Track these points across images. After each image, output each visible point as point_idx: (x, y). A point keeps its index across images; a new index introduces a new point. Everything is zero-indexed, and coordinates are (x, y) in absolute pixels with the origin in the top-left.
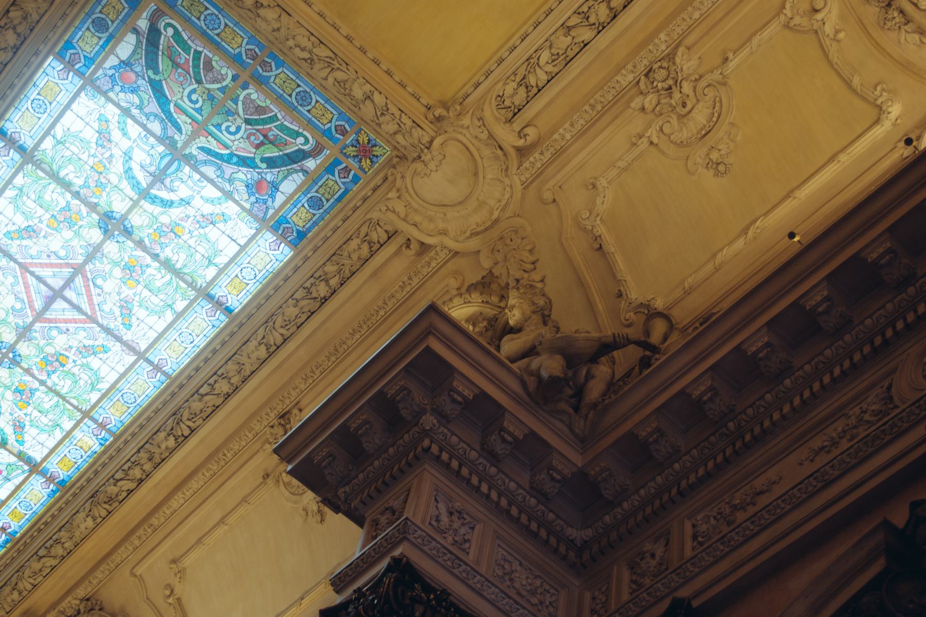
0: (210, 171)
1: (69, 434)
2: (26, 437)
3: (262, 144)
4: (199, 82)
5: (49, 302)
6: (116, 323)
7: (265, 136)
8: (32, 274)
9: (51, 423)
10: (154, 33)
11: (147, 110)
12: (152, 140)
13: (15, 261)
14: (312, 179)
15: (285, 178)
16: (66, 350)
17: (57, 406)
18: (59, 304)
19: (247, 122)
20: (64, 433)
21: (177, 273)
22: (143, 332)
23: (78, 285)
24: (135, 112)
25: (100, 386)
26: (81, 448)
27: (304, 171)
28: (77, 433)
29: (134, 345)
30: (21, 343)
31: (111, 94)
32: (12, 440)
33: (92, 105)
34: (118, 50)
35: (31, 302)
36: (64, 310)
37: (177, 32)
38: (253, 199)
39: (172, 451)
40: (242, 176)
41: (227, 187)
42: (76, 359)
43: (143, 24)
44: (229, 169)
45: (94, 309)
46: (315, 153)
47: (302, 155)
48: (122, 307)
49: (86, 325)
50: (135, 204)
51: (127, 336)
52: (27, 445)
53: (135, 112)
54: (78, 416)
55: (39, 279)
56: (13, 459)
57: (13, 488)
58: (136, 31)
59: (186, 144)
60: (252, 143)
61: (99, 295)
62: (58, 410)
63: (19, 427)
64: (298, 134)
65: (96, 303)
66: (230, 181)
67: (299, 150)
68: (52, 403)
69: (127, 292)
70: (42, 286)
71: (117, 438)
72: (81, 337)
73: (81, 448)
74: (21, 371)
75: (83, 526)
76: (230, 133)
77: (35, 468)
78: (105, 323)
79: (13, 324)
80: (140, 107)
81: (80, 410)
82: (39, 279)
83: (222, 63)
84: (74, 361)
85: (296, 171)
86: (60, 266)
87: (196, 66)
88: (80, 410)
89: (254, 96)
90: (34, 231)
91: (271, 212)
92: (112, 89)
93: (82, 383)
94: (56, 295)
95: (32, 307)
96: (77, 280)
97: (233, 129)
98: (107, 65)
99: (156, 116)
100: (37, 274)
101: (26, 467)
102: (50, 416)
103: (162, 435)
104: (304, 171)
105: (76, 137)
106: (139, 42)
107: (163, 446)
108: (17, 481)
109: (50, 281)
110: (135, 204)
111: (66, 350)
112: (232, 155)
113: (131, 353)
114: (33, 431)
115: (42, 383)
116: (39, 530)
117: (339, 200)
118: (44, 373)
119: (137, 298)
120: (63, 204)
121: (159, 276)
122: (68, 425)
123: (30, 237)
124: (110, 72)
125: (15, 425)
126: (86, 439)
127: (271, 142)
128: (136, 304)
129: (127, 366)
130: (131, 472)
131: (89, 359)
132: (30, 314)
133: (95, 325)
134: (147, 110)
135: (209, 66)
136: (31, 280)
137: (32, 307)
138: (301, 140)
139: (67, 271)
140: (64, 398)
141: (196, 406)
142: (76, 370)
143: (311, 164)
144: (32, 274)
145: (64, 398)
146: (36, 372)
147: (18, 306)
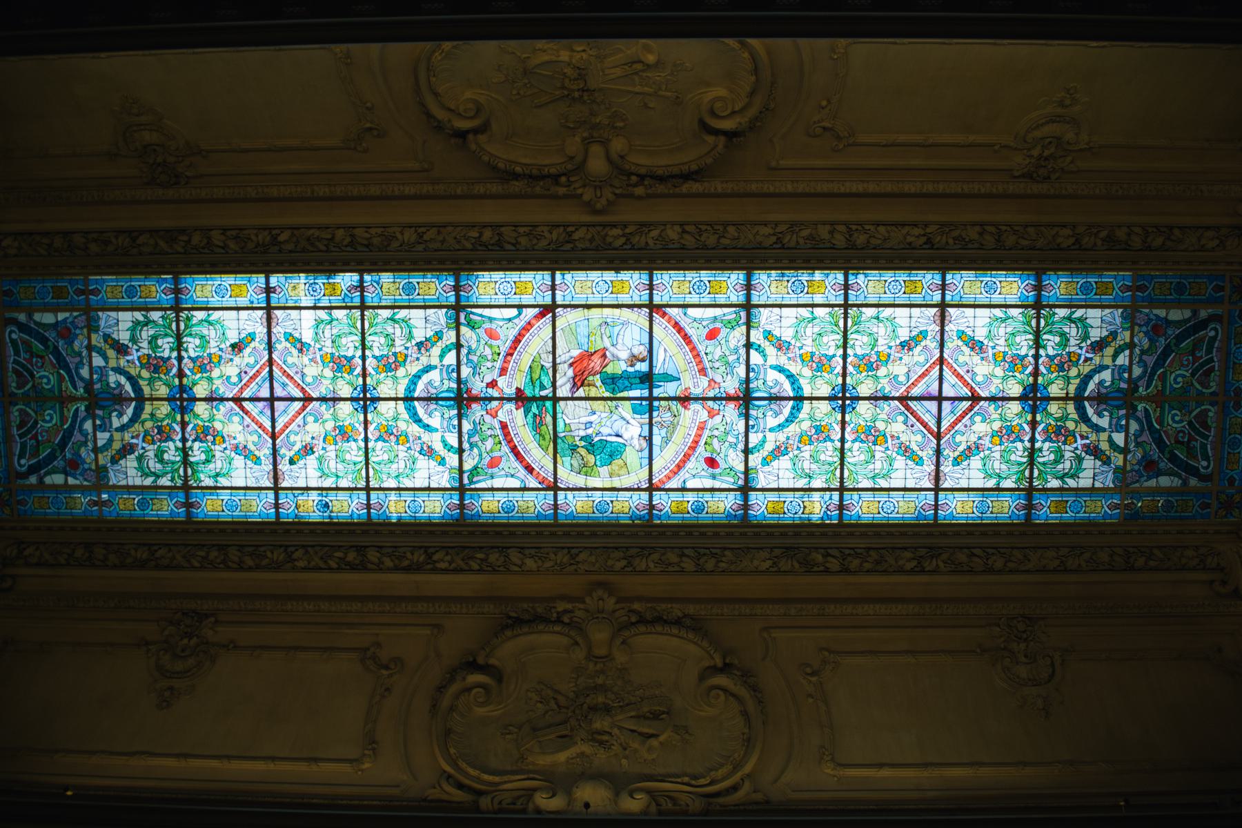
0: (1134, 427)
3: (1182, 443)
4: (1193, 375)
7: (1189, 441)
8: (941, 370)
10: (1203, 324)
11: (1144, 357)
12: (1126, 375)
13: (942, 352)
14: (1183, 491)
15: (1170, 475)
18: (932, 406)
19: (1190, 423)
21: (1031, 463)
24: (1137, 350)
27: (1185, 482)
28: (816, 496)
31: (1136, 328)
33: (1118, 320)
34: (1172, 312)
37: (1214, 339)
38: (1136, 467)
39: (901, 571)
40: (1148, 448)
41: (1132, 446)
43: (1203, 314)
44: (1146, 437)
46: (1202, 478)
47: (1195, 472)
48: (969, 448)
50: (1066, 399)
53: (1137, 350)
54: (836, 484)
55: (941, 379)
56: (741, 468)
58: (1195, 313)
59: (1141, 399)
60: (1176, 437)
62: (827, 467)
64: (1207, 458)
66: (1138, 444)
67: (1198, 469)
69: (986, 442)
70: (937, 383)
71: (841, 524)
72: (915, 439)
75: (756, 563)
76: (1173, 419)
80: (1143, 352)
82: (941, 379)
83: (1217, 379)
84: (887, 449)
85: (1180, 477)
86: (966, 384)
87: (1202, 365)
88: (842, 482)
89: (1211, 414)
90: (981, 348)
91: (1137, 485)
92: (1140, 326)
94: (940, 399)
97: (1177, 418)
98: (1156, 311)
99: (1145, 366)
102: (813, 466)
103: (908, 555)
104: (1185, 482)
105: (1085, 327)
106: (1189, 320)
107: (901, 563)
108: (717, 485)
109: (945, 386)
110: (1066, 399)
111: (892, 436)
112: (1158, 431)
115: (843, 440)
116: (690, 534)
117: (1181, 518)
118: (854, 436)
119: (987, 452)
120: (1023, 352)
121: (1020, 453)
122: (817, 483)
123: (972, 348)
124: (1152, 316)
127: (1188, 448)
128: (982, 455)
130: (849, 559)
134: (1144, 357)
135: (1208, 373)
138: (1204, 463)
141: (962, 557)
143: (1193, 482)
144: (941, 370)
145: (842, 464)
146: (848, 429)
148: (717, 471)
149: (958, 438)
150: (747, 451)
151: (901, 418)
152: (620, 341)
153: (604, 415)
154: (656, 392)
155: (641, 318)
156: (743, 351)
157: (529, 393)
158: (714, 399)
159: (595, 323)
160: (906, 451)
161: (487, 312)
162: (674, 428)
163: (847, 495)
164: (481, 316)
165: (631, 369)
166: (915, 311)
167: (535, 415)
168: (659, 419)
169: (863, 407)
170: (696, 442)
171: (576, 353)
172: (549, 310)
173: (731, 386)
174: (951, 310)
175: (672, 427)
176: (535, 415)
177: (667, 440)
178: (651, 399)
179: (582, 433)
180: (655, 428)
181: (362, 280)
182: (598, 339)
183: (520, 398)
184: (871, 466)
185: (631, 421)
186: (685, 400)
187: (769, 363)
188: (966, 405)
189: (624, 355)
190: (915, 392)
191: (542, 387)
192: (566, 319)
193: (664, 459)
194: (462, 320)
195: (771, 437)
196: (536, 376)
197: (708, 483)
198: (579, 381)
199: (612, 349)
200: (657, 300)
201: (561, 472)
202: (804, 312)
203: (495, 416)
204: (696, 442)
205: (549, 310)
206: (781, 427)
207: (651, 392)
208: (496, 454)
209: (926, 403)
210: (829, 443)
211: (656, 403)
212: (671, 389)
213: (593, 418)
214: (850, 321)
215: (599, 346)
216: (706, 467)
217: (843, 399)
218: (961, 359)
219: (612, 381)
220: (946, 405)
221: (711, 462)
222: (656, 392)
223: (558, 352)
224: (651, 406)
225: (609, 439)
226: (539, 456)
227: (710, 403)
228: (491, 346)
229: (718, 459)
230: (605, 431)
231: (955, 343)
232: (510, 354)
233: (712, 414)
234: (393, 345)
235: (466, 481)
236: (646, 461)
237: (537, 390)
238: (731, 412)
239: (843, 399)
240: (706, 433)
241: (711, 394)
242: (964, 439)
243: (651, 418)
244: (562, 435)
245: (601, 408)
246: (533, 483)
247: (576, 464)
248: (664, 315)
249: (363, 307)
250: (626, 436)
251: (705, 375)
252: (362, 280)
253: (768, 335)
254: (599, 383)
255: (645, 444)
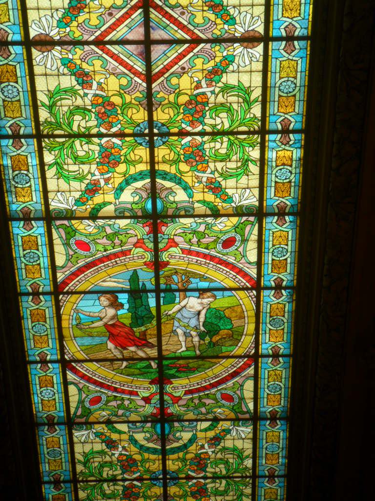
1: (262, 161)
2: (230, 192)
5: (147, 58)
6: (219, 27)
8: (112, 43)
9: (239, 164)
13: (88, 43)
16: (197, 87)
17: (232, 145)
18: (157, 51)
20: (258, 164)
22: (249, 16)
23: (157, 20)
25: (253, 97)
26: (284, 164)
28: (271, 155)
29: (252, 34)
30: (155, 113)
32: (220, 205)
35: (131, 69)
36: (164, 53)
42: (212, 89)
45: (189, 30)
49: (195, 51)
51: (239, 31)
52: (236, 198)
55: (123, 42)
56: (235, 220)
57: (255, 245)
61: (183, 13)
62: (235, 148)
63: (215, 188)
65: (186, 23)
68: (225, 145)
70: (128, 47)
73: (284, 164)
74: (176, 138)
77: (260, 213)
78: (210, 36)
79: (133, 101)
81: (254, 133)
82: (123, 42)
84: (213, 92)
86: (127, 15)
88: (254, 133)
93: (235, 106)
94: (147, 43)
95: (136, 73)
96: (152, 16)
100: (114, 39)
101: (252, 219)
108: (254, 236)
109: (130, 37)
113: (256, 44)
114: (231, 182)
115: (202, 134)
122: (255, 154)
125: (210, 188)
126: (281, 154)
129: (261, 59)
131: (224, 80)
132: (140, 82)
133: (202, 45)
136: (115, 49)
137: (136, 73)
139: (138, 15)
140: (232, 133)
142: (220, 99)
144: (112, 43)
145: (232, 133)
146: (189, 129)
147: (124, 81)
148: (238, 237)
149: (199, 20)
150: (216, 214)
151: (174, 81)
152: (97, 314)
153: (176, 324)
154: (150, 286)
155: (69, 305)
156: (100, 222)
157: (155, 376)
158: (156, 242)
159: (78, 332)
160: (215, 73)
161: (73, 405)
162: (190, 272)
163: (270, 126)
164: (77, 408)
165: (126, 306)
166: (37, 70)
167: (178, 371)
168: (180, 285)
169: (161, 116)
170: (205, 256)
171: (110, 345)
172: (66, 364)
173: (141, 231)
174: (33, 34)
175: (189, 275)
176: (178, 371)
177: (203, 278)
178: (157, 291)
179: (196, 339)
180: (191, 286)
181: (49, 483)
182: (95, 330)
183: (162, 380)
184: (235, 106)
185: (183, 304)
186: (157, 265)
187: (113, 200)
188: (154, 14)
189: (111, 312)
190: (140, 66)
191: (150, 366)
192: (73, 349)
193: (221, 277)
194: (83, 420)
195: (198, 196)
196: (137, 372)
197: (252, 246)
198: (142, 342)
199: (105, 320)
200: (49, 288)
201: (239, 351)
202: (50, 173)
203: (180, 398)
204: (205, 256)
205: (66, 364)
206: (186, 188)
207: (151, 291)
208: (219, 396)
209: (154, 56)
210: (206, 146)
211: (163, 286)
212: (147, 278)
213: (180, 331)
214: (57, 132)
215: (104, 330)
216: (233, 248)
217: (151, 135)
218: (94, 21)
219: (138, 319)
220: (156, 35)
221: (228, 243)
222: (150, 286)
223: (110, 356)
224: (165, 291)
225: (202, 319)
226: (221, 368)
227: (161, 246)
228: (108, 402)
229: (224, 238)
230: (193, 322)
231: (74, 29)
232: (115, 390)
233: (172, 243)
234: (111, 462)
235: (247, 416)
236: (227, 293)
237: (152, 370)
238: (170, 230)
239: (151, 135)
240: (195, 248)
241: (151, 245)
242: (199, 15)
243: (179, 290)
244: (198, 352)
245: (168, 326)
246: (251, 371)
247: (231, 343)
248: (65, 283)
249: (74, 481)
250: (199, 308)
251: (130, 250)
252: (49, 483)
253: (80, 201)
254: (143, 329)
255: (209, 294)
